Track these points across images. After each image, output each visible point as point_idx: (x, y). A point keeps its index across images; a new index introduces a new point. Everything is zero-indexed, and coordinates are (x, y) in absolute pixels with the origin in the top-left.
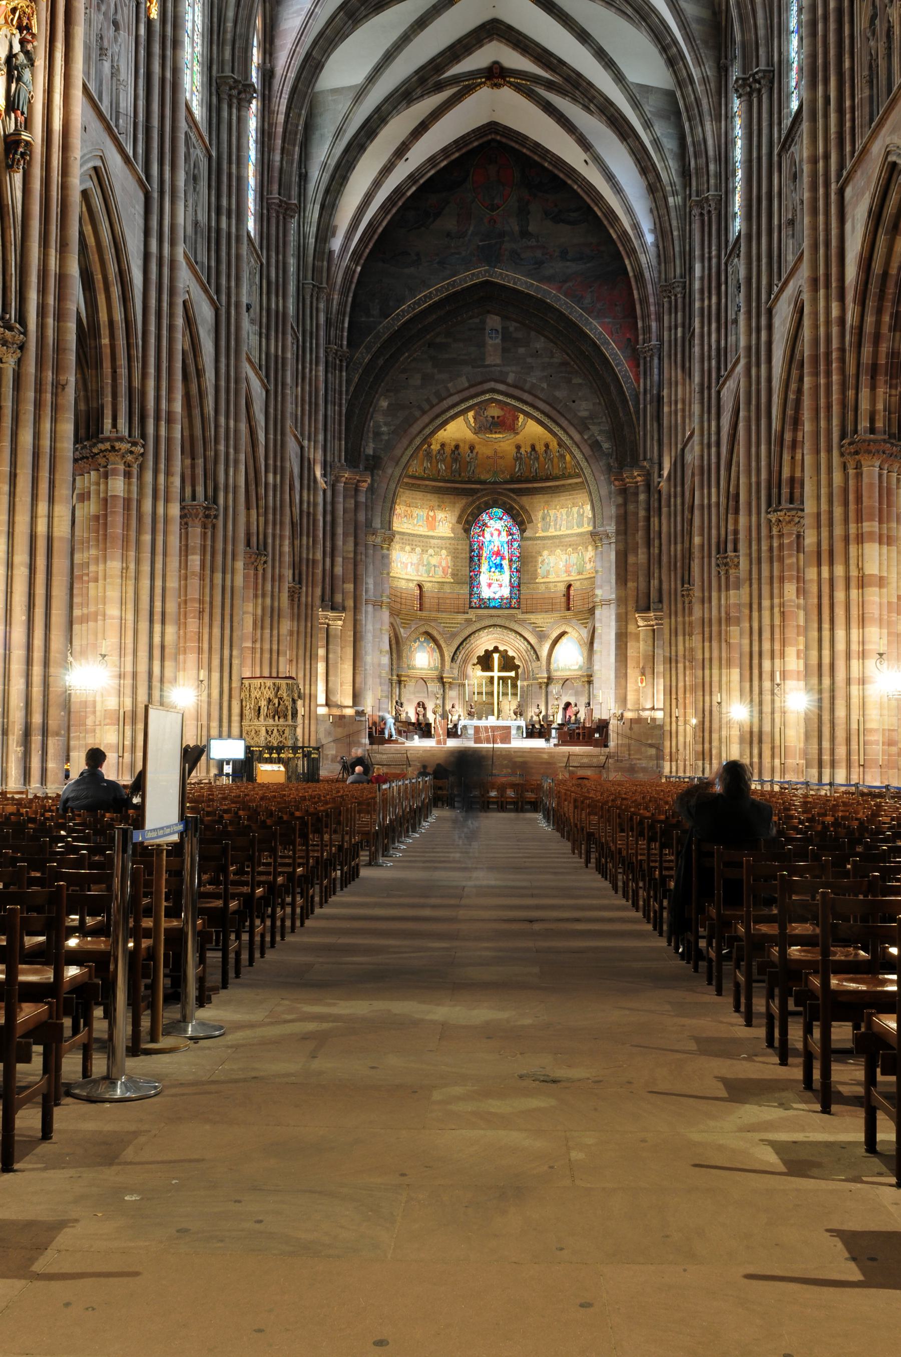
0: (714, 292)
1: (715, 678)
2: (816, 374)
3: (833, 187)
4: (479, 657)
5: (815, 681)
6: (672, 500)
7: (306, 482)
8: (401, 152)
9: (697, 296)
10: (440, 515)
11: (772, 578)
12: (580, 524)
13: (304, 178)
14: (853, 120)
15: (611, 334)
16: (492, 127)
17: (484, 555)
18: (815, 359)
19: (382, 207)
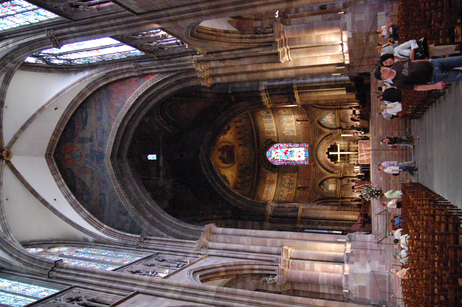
4: (331, 161)
6: (171, 17)
7: (160, 293)
10: (268, 178)
12: (270, 117)
15: (133, 91)
16: (47, 156)
17: (286, 159)
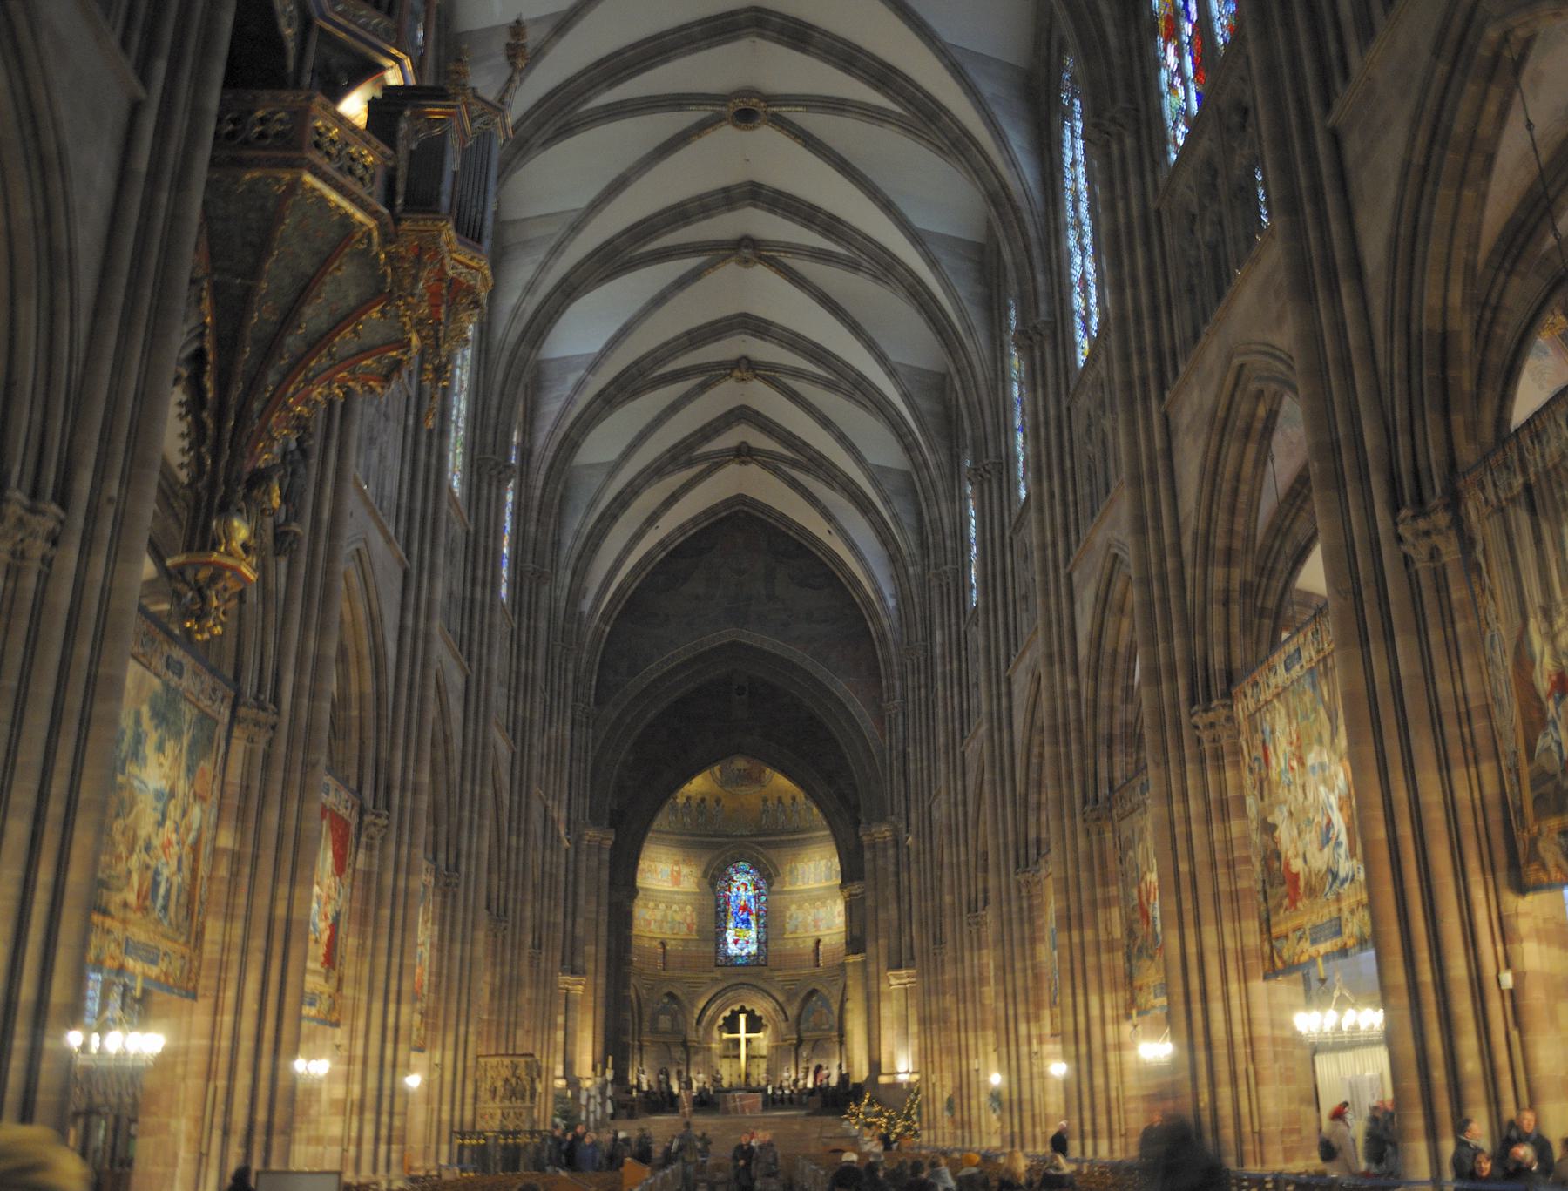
0: (955, 656)
1: (972, 1042)
2: (1056, 743)
3: (1062, 571)
4: (725, 1018)
5: (1072, 1049)
8: (652, 520)
9: (939, 661)
10: (685, 870)
11: (1023, 939)
12: (828, 878)
13: (557, 545)
14: (1076, 512)
16: (740, 499)
18: (1054, 729)
19: (632, 571)
